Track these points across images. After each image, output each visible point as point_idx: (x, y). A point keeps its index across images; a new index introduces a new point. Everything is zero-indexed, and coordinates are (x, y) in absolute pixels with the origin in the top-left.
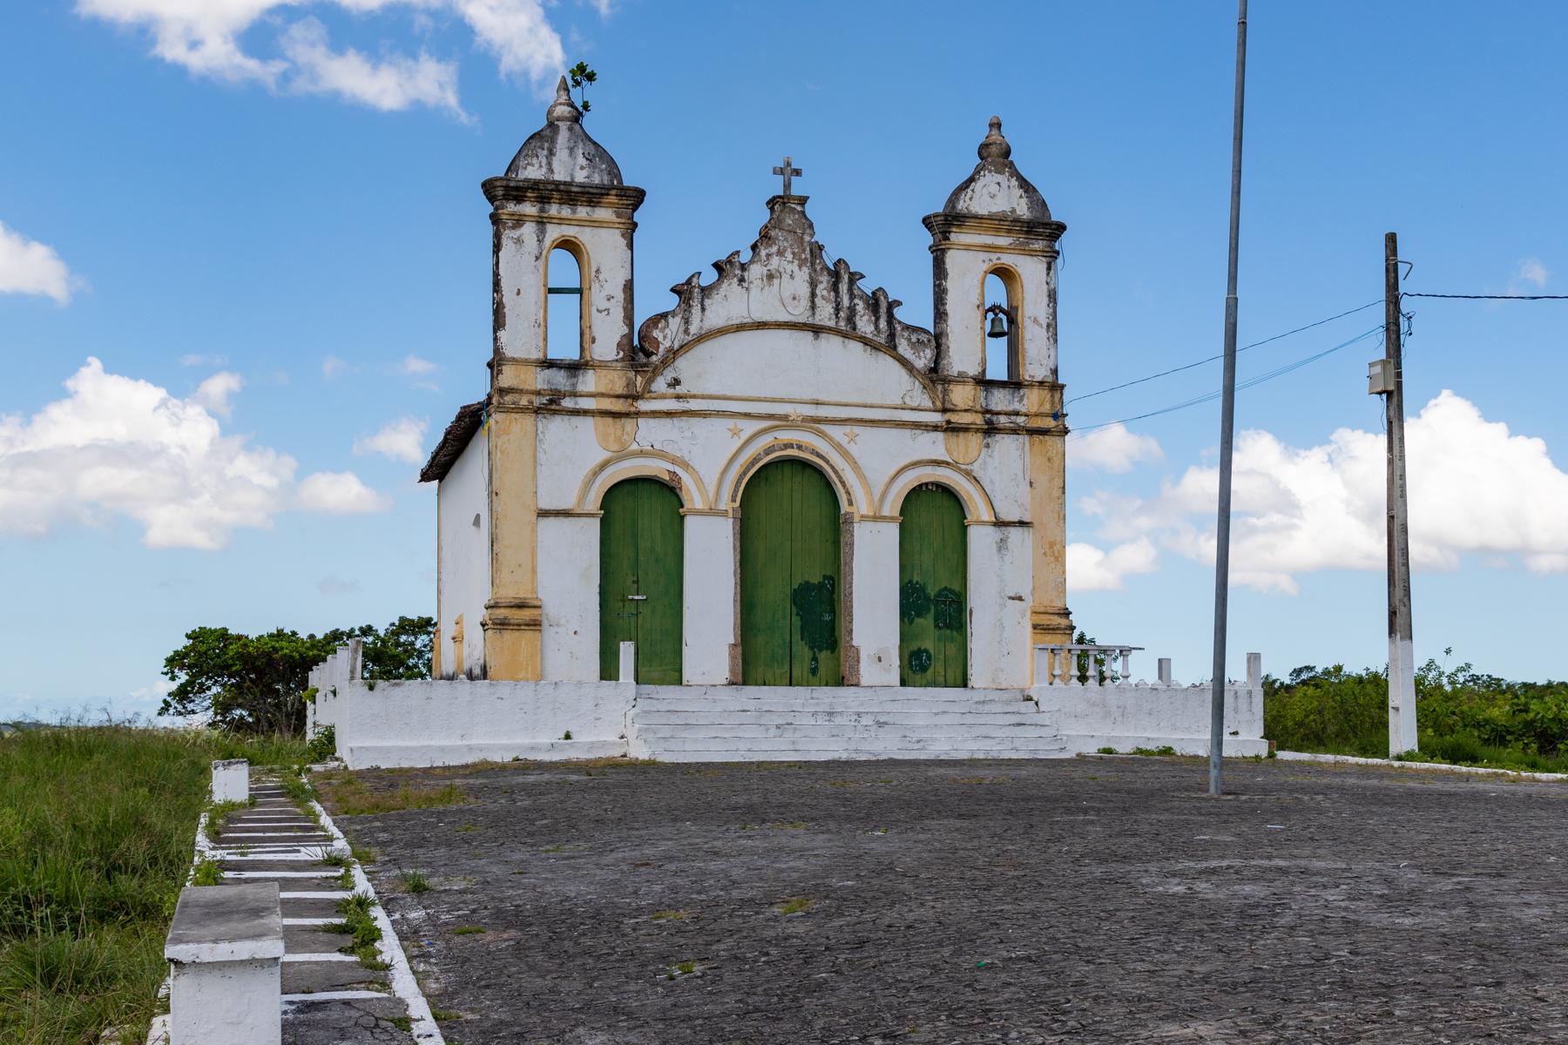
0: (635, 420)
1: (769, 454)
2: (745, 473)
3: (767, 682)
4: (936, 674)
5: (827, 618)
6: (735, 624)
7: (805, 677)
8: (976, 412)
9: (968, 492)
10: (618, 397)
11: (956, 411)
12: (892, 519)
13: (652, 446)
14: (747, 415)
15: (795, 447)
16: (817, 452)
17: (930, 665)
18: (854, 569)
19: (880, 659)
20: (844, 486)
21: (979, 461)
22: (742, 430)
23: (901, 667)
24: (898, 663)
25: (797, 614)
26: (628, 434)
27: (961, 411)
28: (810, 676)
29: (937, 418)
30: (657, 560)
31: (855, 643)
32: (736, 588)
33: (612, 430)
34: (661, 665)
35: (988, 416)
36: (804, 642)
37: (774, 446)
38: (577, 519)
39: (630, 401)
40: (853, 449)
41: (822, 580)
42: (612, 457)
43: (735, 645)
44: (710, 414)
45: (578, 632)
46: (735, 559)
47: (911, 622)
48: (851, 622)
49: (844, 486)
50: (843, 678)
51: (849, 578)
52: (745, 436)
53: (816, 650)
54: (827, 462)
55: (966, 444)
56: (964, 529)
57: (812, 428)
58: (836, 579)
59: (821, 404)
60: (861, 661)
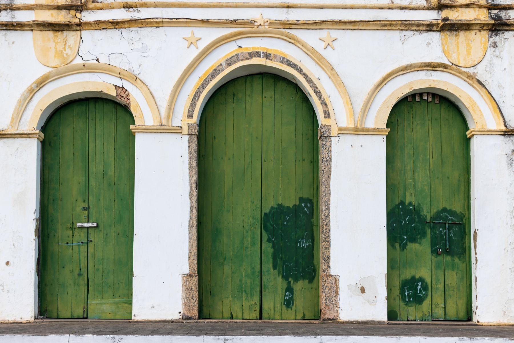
0: (79, 32)
1: (230, 65)
2: (203, 86)
3: (234, 316)
4: (434, 306)
5: (304, 244)
6: (190, 252)
7: (278, 309)
8: (480, 7)
9: (470, 98)
10: (59, 8)
11: (455, 7)
12: (376, 131)
13: (97, 60)
14: (205, 22)
15: (262, 55)
16: (288, 61)
17: (427, 295)
18: (331, 188)
19: (363, 290)
20: (320, 96)
21: (485, 62)
22: (200, 39)
23: (389, 298)
24: (383, 293)
25: (269, 240)
26: (70, 47)
27: (461, 6)
28: (284, 307)
29: (433, 16)
30: (110, 185)
31: (332, 272)
32: (191, 212)
33: (52, 44)
34: (114, 297)
35: (495, 12)
36: (276, 271)
37: (237, 55)
38: (11, 140)
39: (73, 12)
40: (329, 55)
41: (298, 203)
42: (50, 72)
43: (190, 275)
44: (163, 22)
45: (11, 262)
46: (190, 180)
47: (403, 247)
48: (328, 248)
49: (320, 96)
50: (321, 310)
51: (325, 199)
52: (202, 45)
53: (290, 279)
54: (300, 71)
55: (468, 45)
56: (467, 141)
57: (282, 34)
58: (315, 204)
59: (291, 7)
60: (340, 292)
